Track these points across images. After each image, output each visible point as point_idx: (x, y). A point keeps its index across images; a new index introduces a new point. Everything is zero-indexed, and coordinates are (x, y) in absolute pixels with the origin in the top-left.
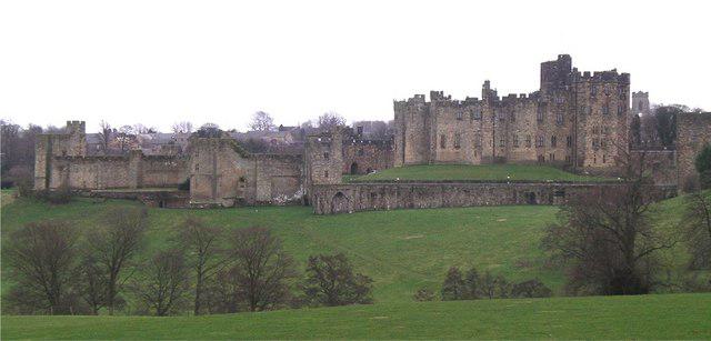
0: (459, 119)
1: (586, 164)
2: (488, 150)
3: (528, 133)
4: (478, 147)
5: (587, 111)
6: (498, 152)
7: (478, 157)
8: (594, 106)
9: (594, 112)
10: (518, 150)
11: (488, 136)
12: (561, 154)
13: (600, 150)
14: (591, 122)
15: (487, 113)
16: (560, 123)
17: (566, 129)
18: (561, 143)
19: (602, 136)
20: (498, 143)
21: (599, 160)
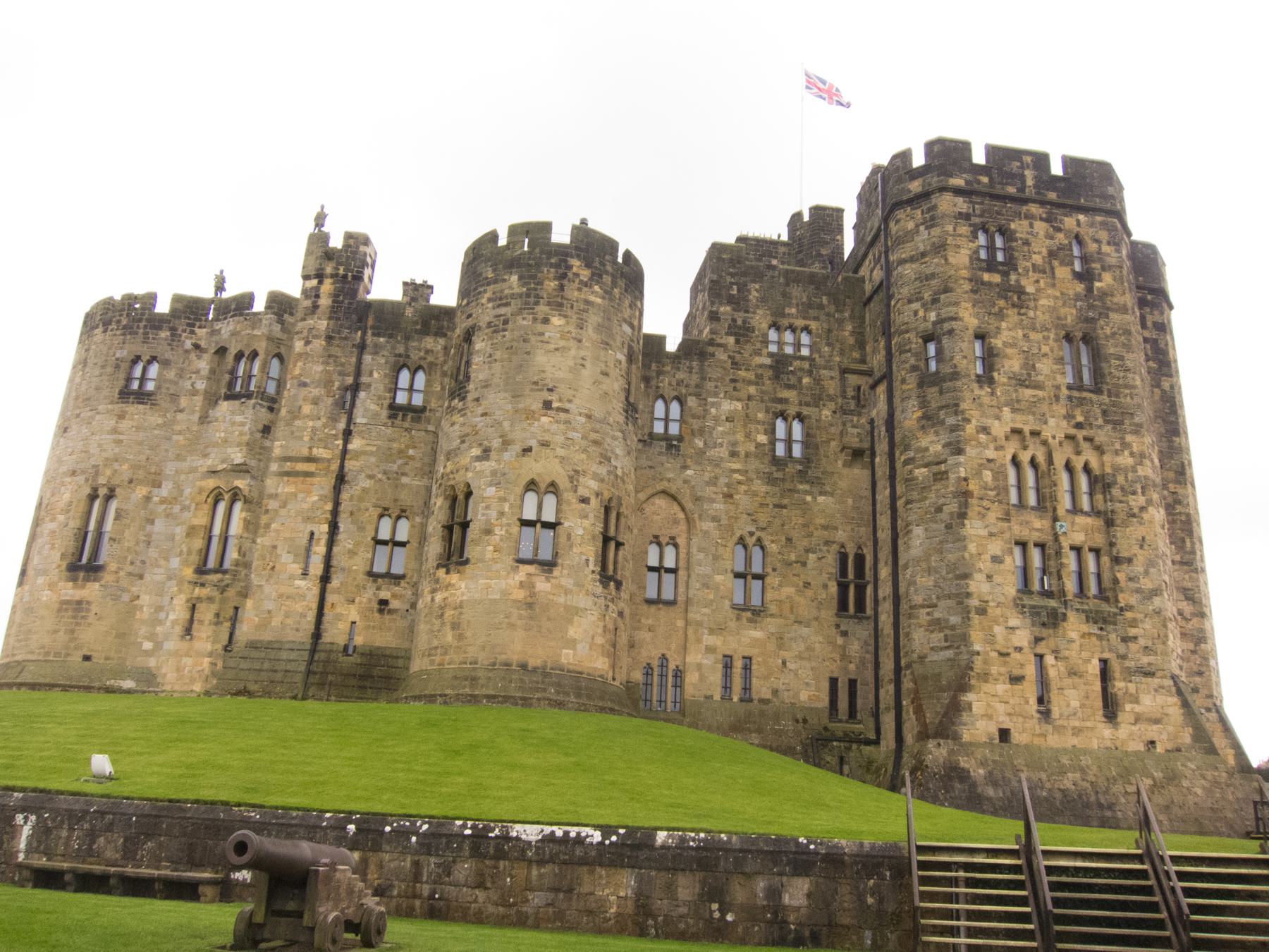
0: (142, 397)
1: (978, 726)
2: (279, 605)
3: (544, 467)
4: (219, 573)
5: (967, 355)
6: (350, 622)
7: (207, 639)
8: (1007, 334)
9: (1011, 364)
10: (462, 587)
11: (297, 508)
12: (800, 663)
13: (1075, 626)
14: (991, 432)
15: (311, 366)
16: (791, 475)
17: (834, 505)
18: (805, 591)
19: (1078, 530)
20: (354, 557)
21: (1076, 699)
